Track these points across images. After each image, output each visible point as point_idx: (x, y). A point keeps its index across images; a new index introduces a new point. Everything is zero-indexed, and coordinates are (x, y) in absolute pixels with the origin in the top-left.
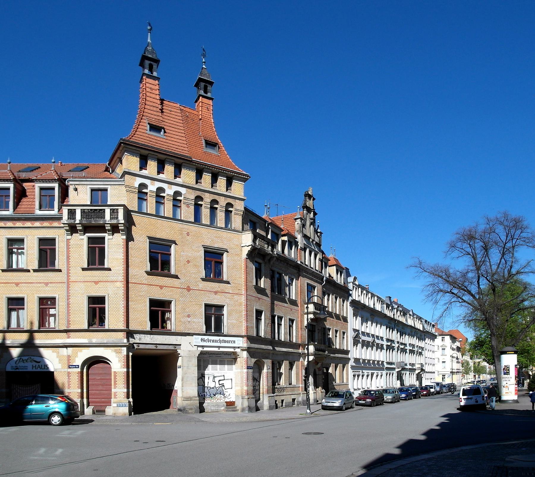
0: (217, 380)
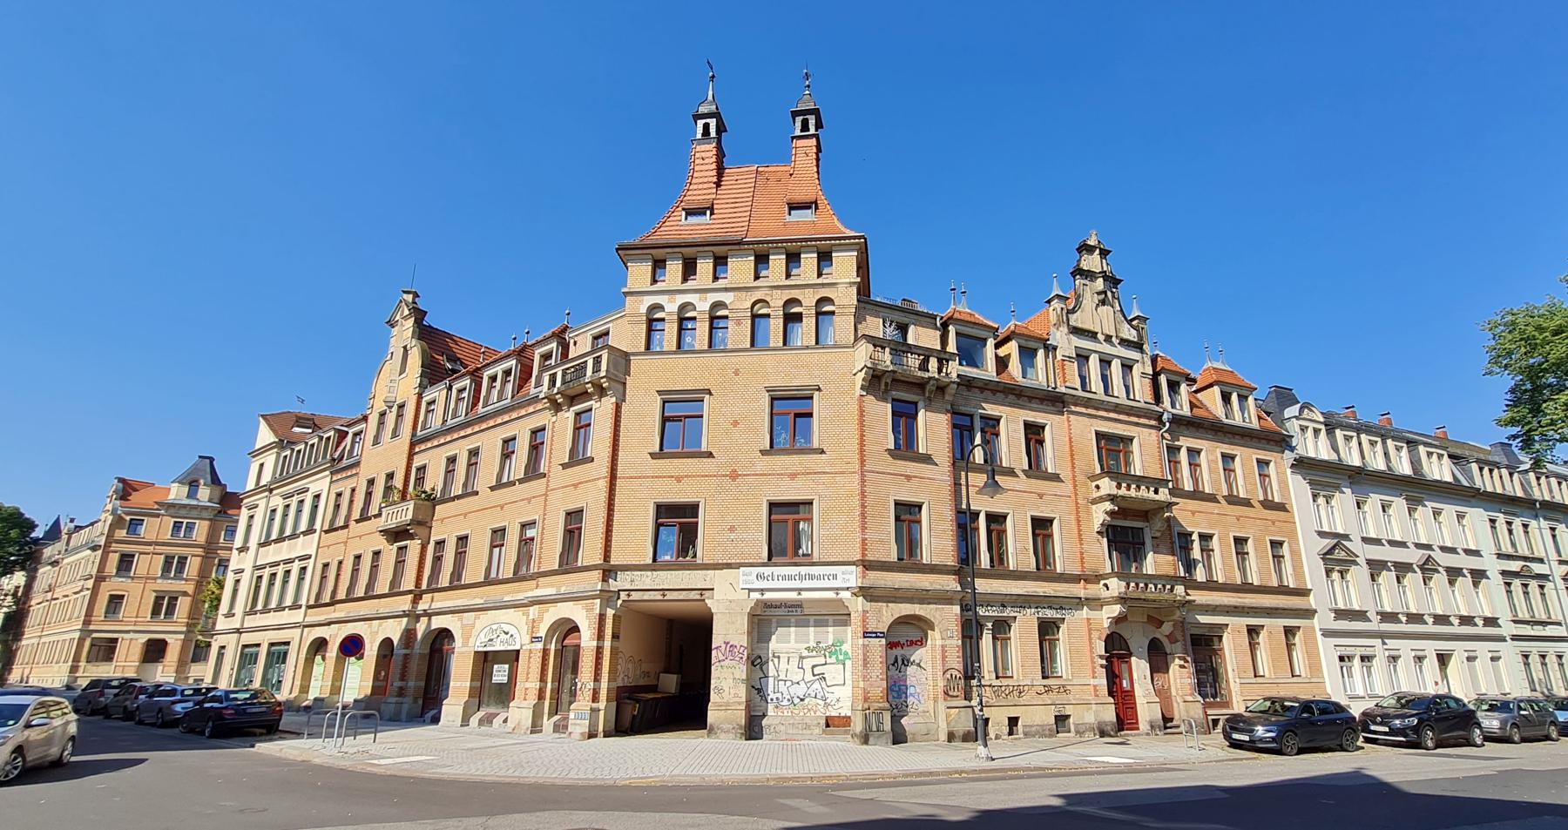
0: (807, 664)
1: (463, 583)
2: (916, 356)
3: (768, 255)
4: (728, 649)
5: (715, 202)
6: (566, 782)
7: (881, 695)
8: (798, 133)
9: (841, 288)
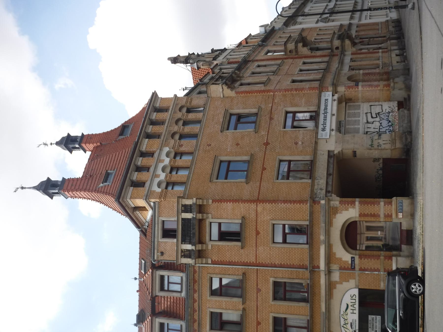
0: (370, 120)
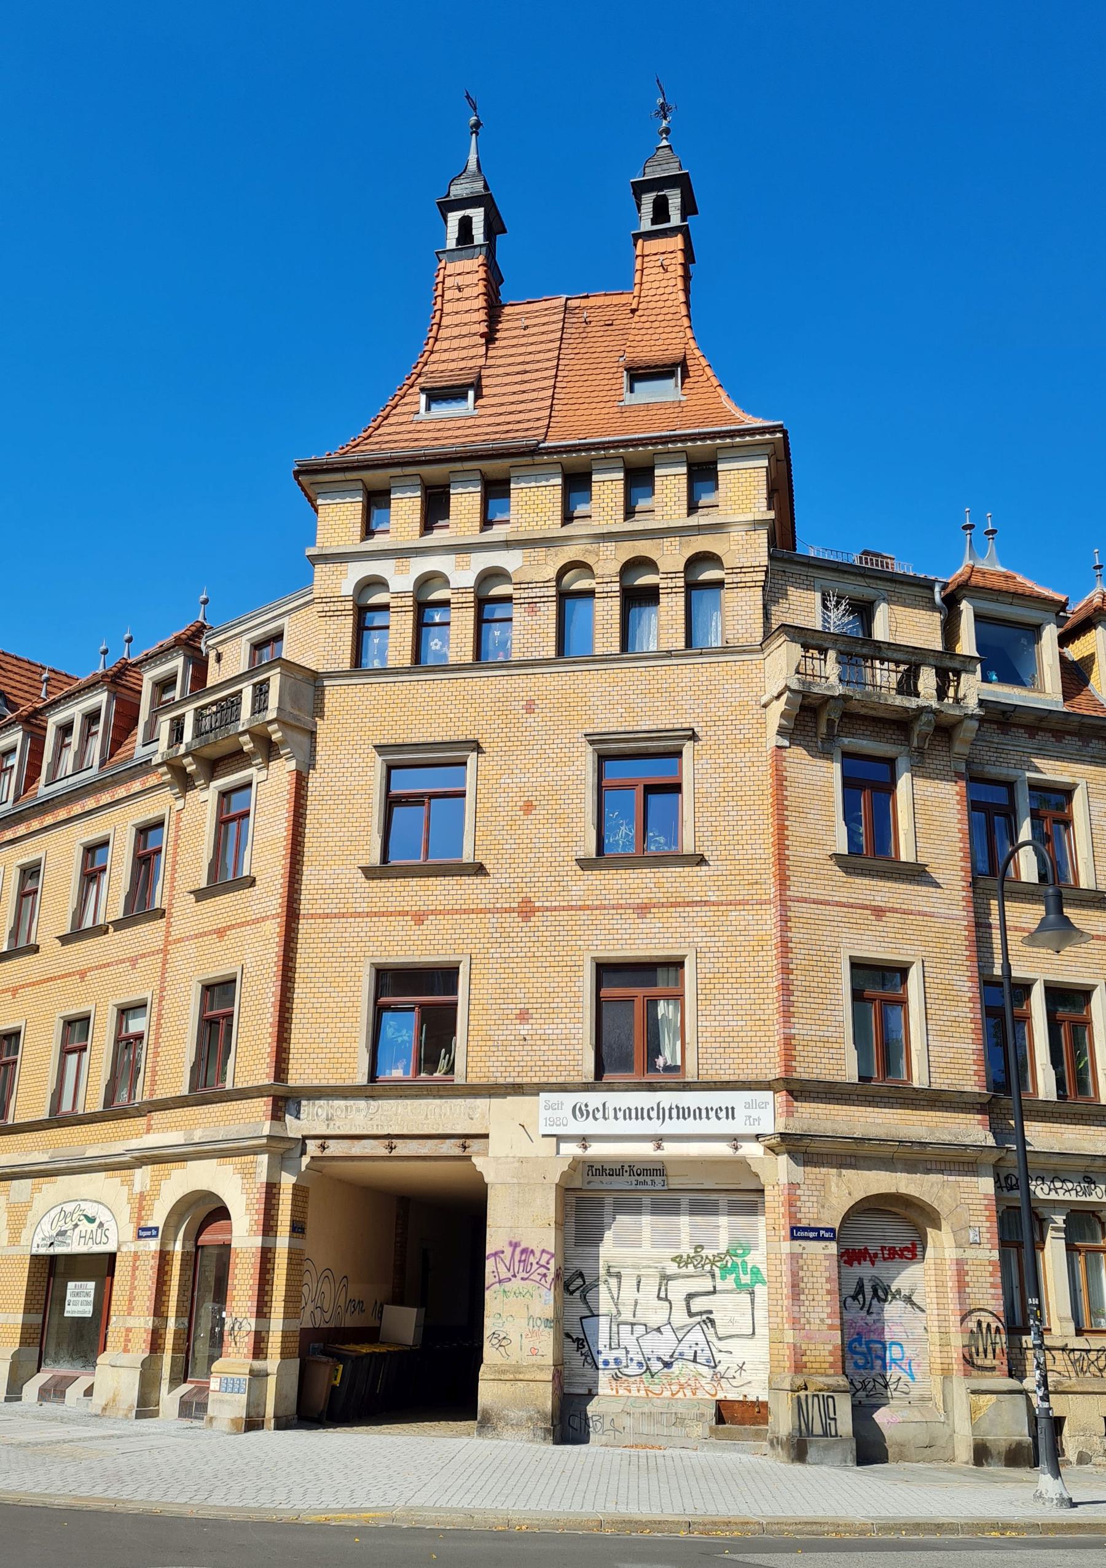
0: (678, 1290)
1: (10, 1122)
2: (892, 666)
3: (590, 474)
4: (517, 1258)
5: (484, 372)
6: (203, 1514)
7: (831, 1359)
8: (646, 225)
9: (737, 535)
